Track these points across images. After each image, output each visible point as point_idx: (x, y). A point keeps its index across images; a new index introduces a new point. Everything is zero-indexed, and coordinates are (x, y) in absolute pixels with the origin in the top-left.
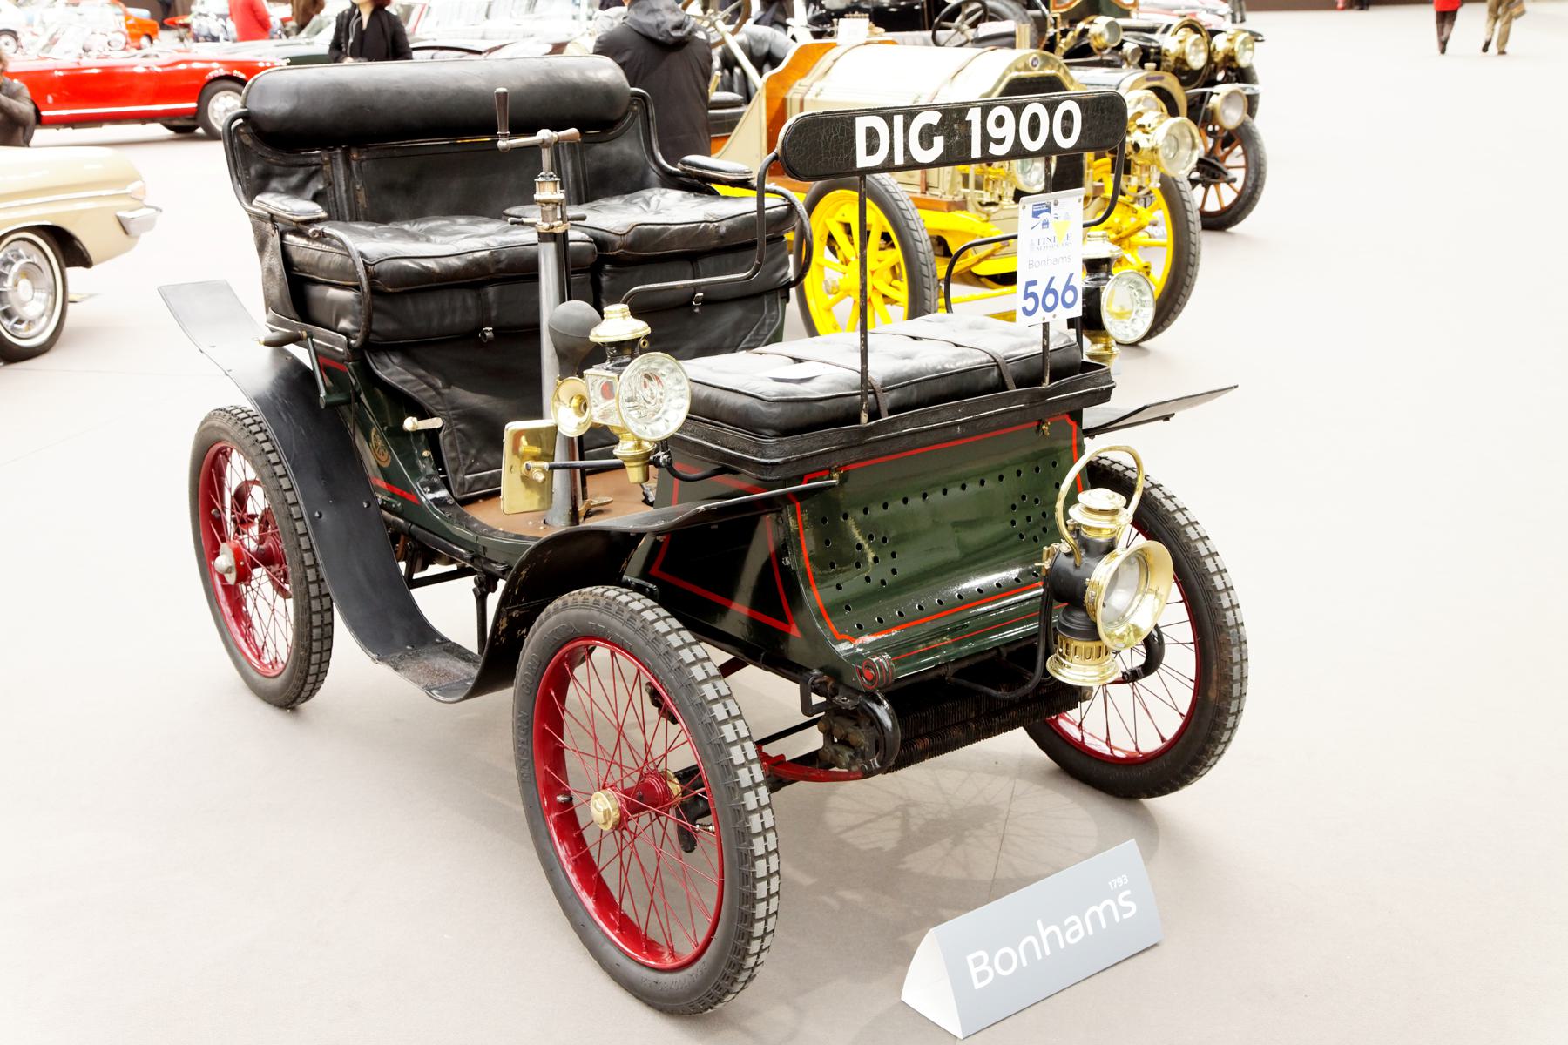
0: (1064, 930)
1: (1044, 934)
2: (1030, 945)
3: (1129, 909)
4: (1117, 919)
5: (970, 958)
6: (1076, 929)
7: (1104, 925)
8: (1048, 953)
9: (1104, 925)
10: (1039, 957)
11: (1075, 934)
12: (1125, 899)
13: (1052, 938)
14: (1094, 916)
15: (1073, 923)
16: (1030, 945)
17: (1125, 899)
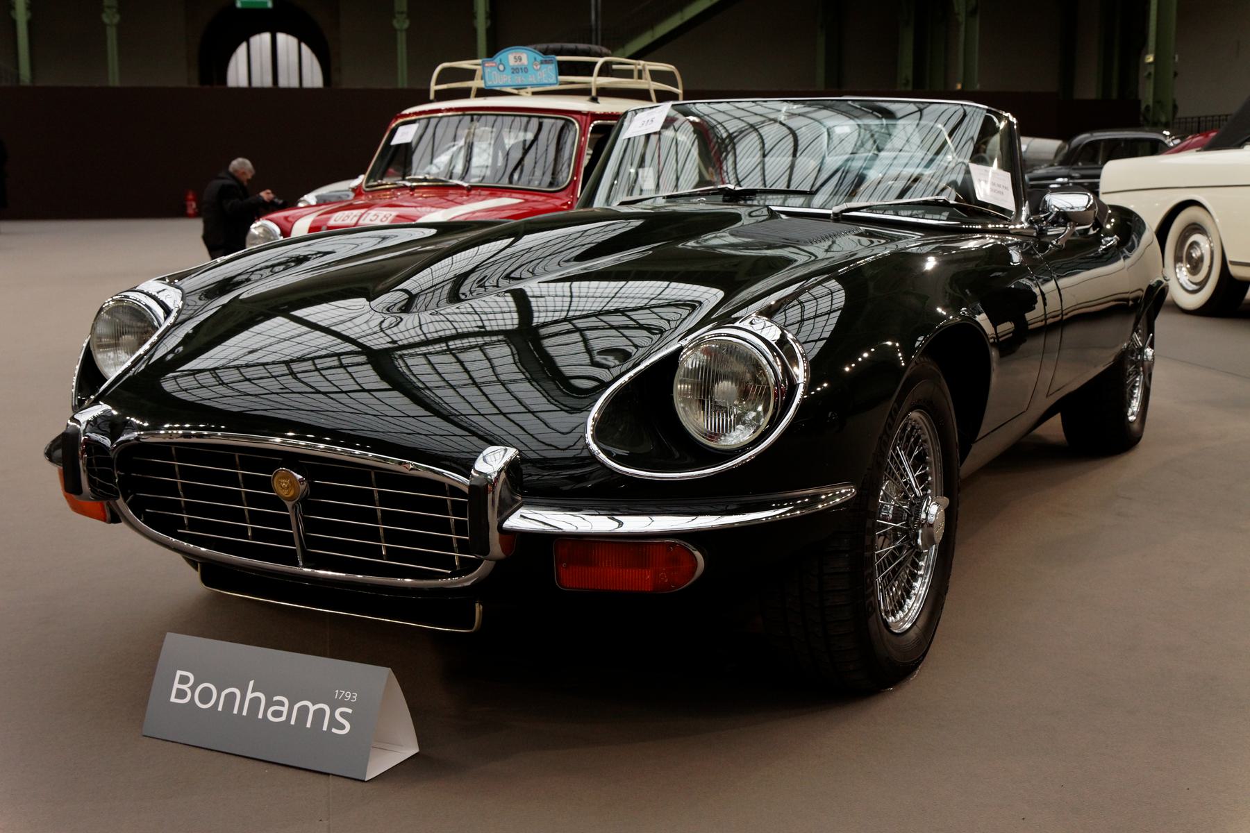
0: (270, 703)
1: (250, 695)
2: (231, 698)
4: (325, 728)
6: (281, 711)
7: (308, 725)
8: (245, 713)
9: (308, 725)
10: (235, 712)
11: (277, 714)
12: (342, 714)
13: (256, 701)
14: (304, 710)
15: (282, 704)
16: (233, 694)
17: (342, 714)
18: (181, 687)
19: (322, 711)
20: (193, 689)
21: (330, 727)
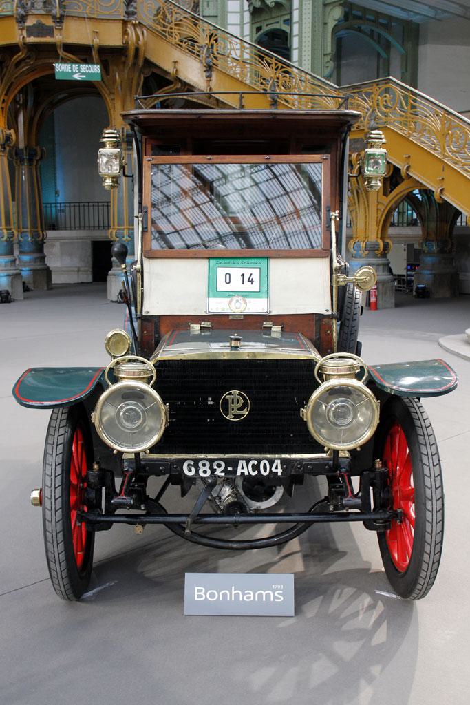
1: (233, 592)
2: (225, 595)
3: (280, 599)
4: (272, 600)
5: (196, 588)
6: (250, 596)
7: (264, 600)
8: (233, 599)
9: (264, 600)
11: (247, 598)
12: (278, 594)
13: (237, 595)
14: (260, 596)
17: (278, 594)
18: (199, 593)
19: (269, 594)
20: (205, 593)
21: (274, 599)
